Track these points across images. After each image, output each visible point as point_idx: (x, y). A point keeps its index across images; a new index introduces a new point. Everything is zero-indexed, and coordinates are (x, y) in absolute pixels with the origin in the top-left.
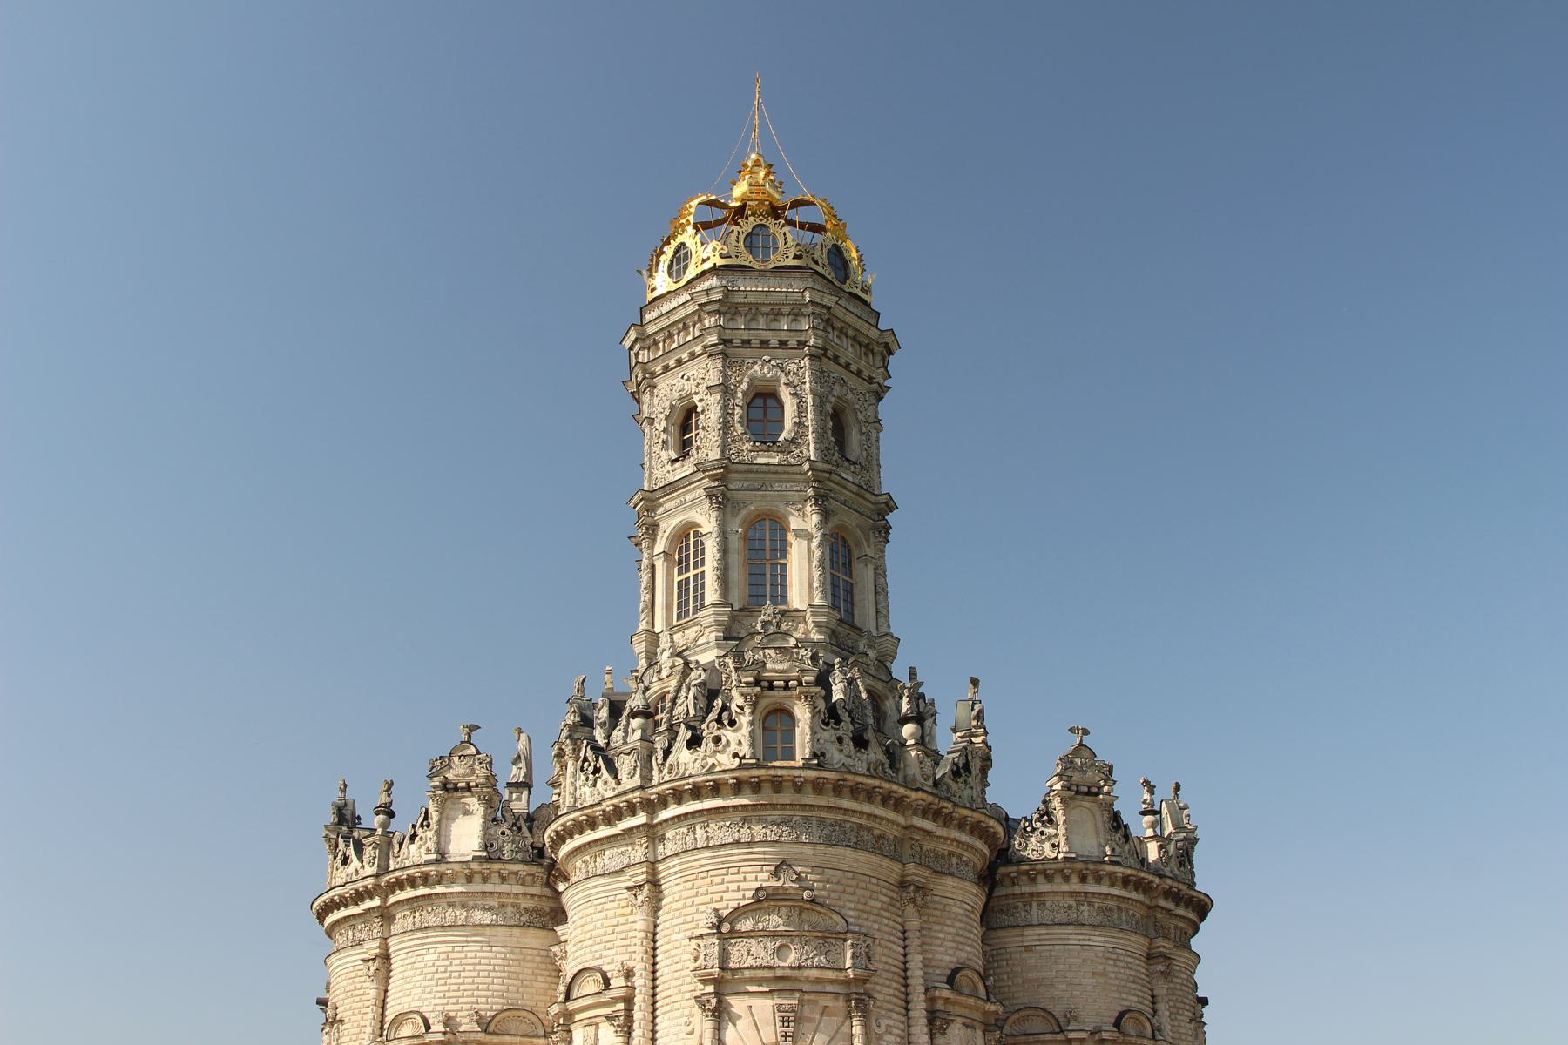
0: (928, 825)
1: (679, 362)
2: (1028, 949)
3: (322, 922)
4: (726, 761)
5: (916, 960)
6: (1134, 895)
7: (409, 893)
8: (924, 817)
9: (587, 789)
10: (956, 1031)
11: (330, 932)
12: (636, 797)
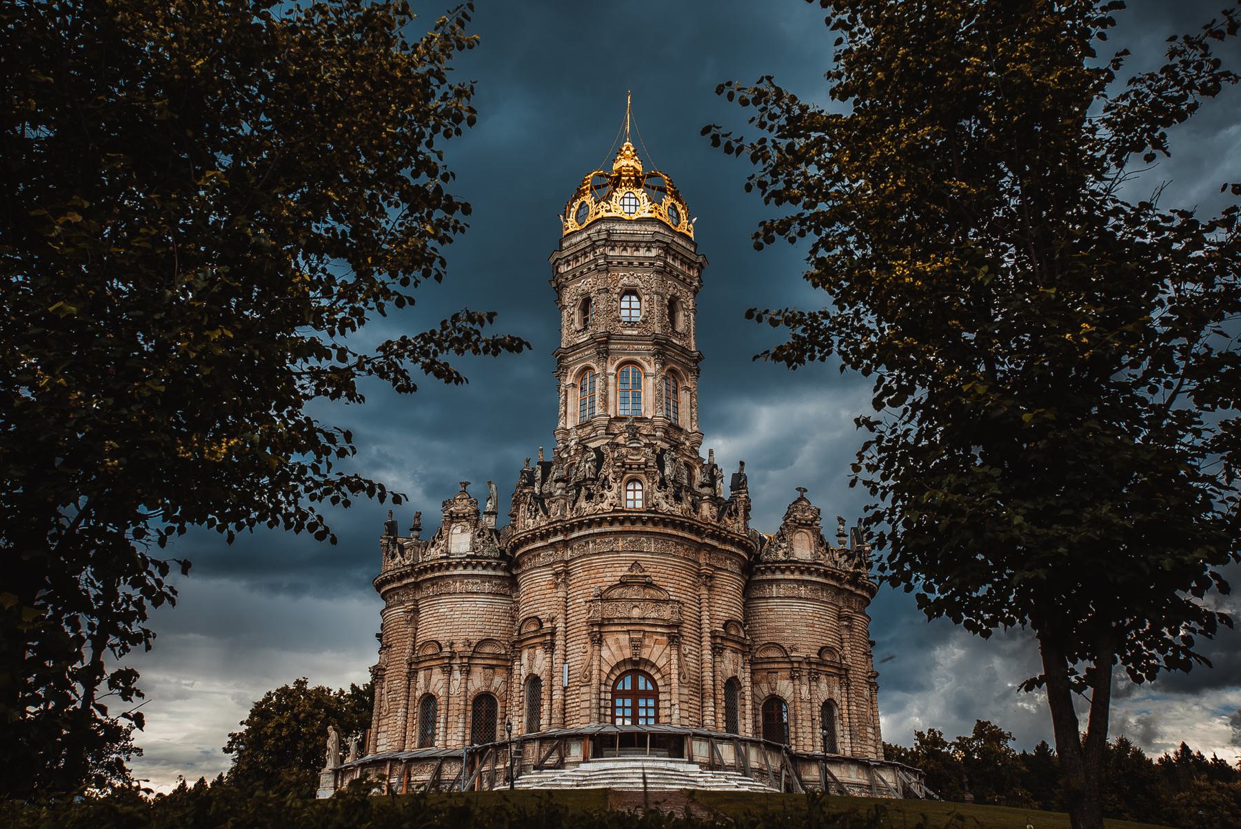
2: (770, 610)
3: (379, 591)
4: (605, 505)
6: (831, 583)
8: (712, 538)
10: (728, 654)
11: (383, 596)
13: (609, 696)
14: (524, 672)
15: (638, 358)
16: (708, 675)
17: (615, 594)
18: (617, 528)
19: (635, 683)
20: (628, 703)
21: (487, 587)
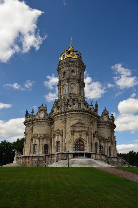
0: (93, 116)
1: (64, 67)
4: (74, 108)
5: (92, 130)
7: (36, 121)
9: (57, 111)
12: (64, 112)
13: (75, 145)
14: (56, 140)
15: (75, 83)
16: (93, 141)
17: (76, 125)
18: (76, 112)
19: (80, 143)
20: (78, 147)
21: (47, 124)
